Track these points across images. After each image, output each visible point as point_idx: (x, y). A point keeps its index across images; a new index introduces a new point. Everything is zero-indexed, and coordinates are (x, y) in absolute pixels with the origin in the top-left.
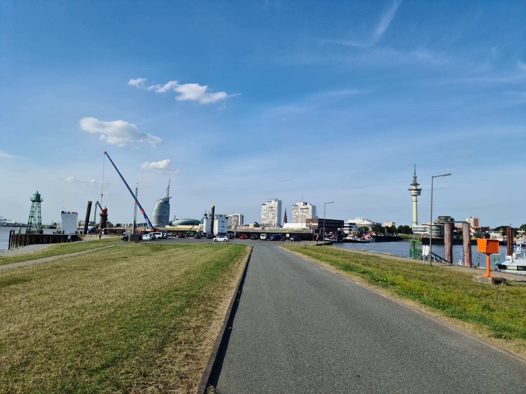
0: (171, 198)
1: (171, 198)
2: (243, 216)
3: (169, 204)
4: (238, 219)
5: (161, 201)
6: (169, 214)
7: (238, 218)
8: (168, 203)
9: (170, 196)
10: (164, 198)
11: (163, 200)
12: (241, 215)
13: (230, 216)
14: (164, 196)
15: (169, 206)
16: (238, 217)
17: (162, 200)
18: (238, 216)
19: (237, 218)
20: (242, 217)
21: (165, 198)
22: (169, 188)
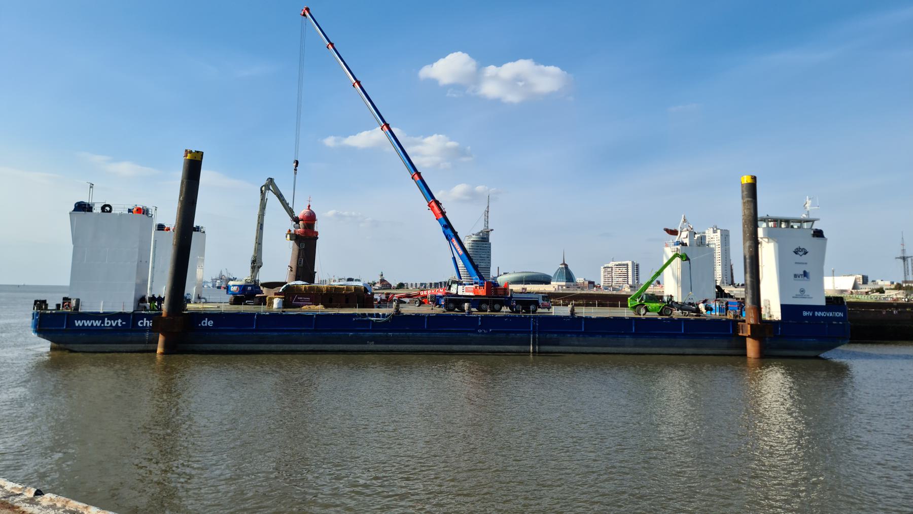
0: (492, 230)
1: (492, 230)
2: (637, 266)
3: (490, 244)
4: (627, 271)
5: (474, 238)
6: (490, 263)
7: (627, 269)
8: (489, 241)
9: (490, 228)
10: (480, 231)
11: (478, 234)
12: (633, 263)
13: (610, 265)
14: (480, 228)
15: (490, 247)
16: (627, 267)
17: (477, 235)
18: (627, 265)
19: (624, 270)
20: (636, 267)
21: (482, 232)
22: (488, 212)
